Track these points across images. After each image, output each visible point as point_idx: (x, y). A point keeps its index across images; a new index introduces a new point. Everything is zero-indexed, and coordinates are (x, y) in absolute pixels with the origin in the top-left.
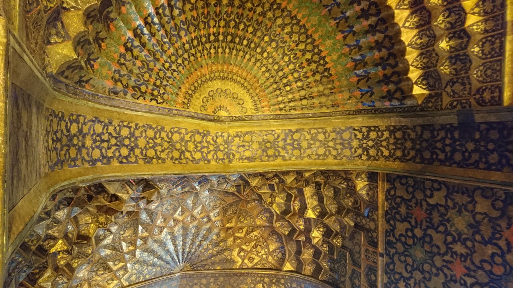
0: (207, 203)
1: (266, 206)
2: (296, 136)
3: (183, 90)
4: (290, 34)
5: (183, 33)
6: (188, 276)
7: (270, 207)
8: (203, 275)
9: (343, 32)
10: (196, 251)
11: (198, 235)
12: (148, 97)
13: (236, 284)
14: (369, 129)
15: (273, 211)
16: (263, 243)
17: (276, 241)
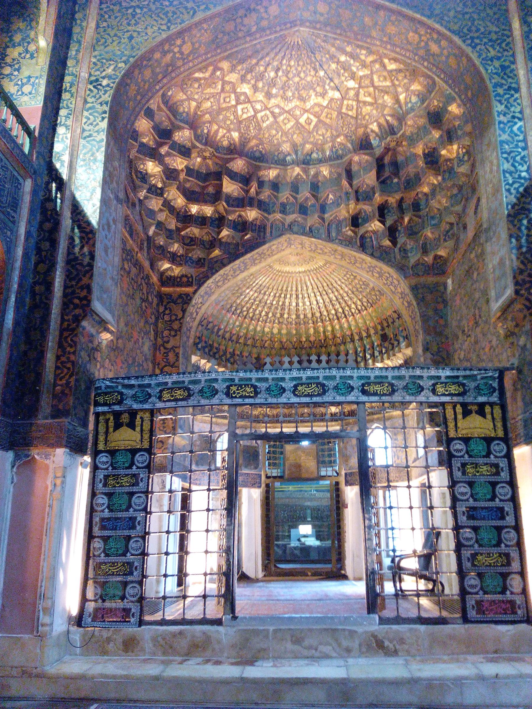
0: (280, 134)
1: (209, 148)
2: (238, 272)
3: (330, 270)
4: (261, 312)
5: (334, 298)
6: (288, 25)
7: (203, 147)
8: (268, 32)
9: (234, 335)
10: (281, 63)
11: (282, 88)
12: (358, 277)
13: (219, 37)
14: (197, 315)
15: (198, 144)
16: (192, 92)
17: (176, 103)
